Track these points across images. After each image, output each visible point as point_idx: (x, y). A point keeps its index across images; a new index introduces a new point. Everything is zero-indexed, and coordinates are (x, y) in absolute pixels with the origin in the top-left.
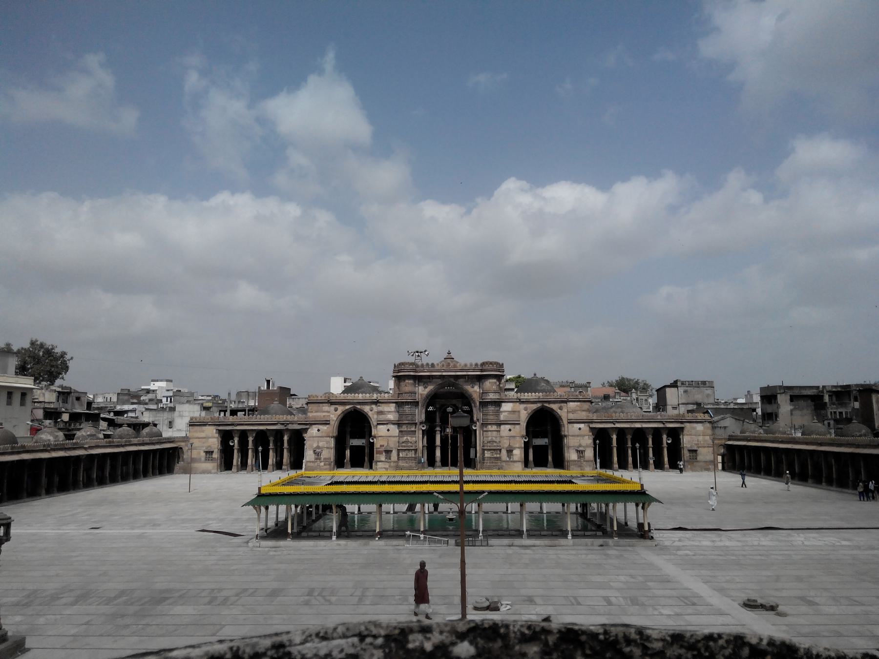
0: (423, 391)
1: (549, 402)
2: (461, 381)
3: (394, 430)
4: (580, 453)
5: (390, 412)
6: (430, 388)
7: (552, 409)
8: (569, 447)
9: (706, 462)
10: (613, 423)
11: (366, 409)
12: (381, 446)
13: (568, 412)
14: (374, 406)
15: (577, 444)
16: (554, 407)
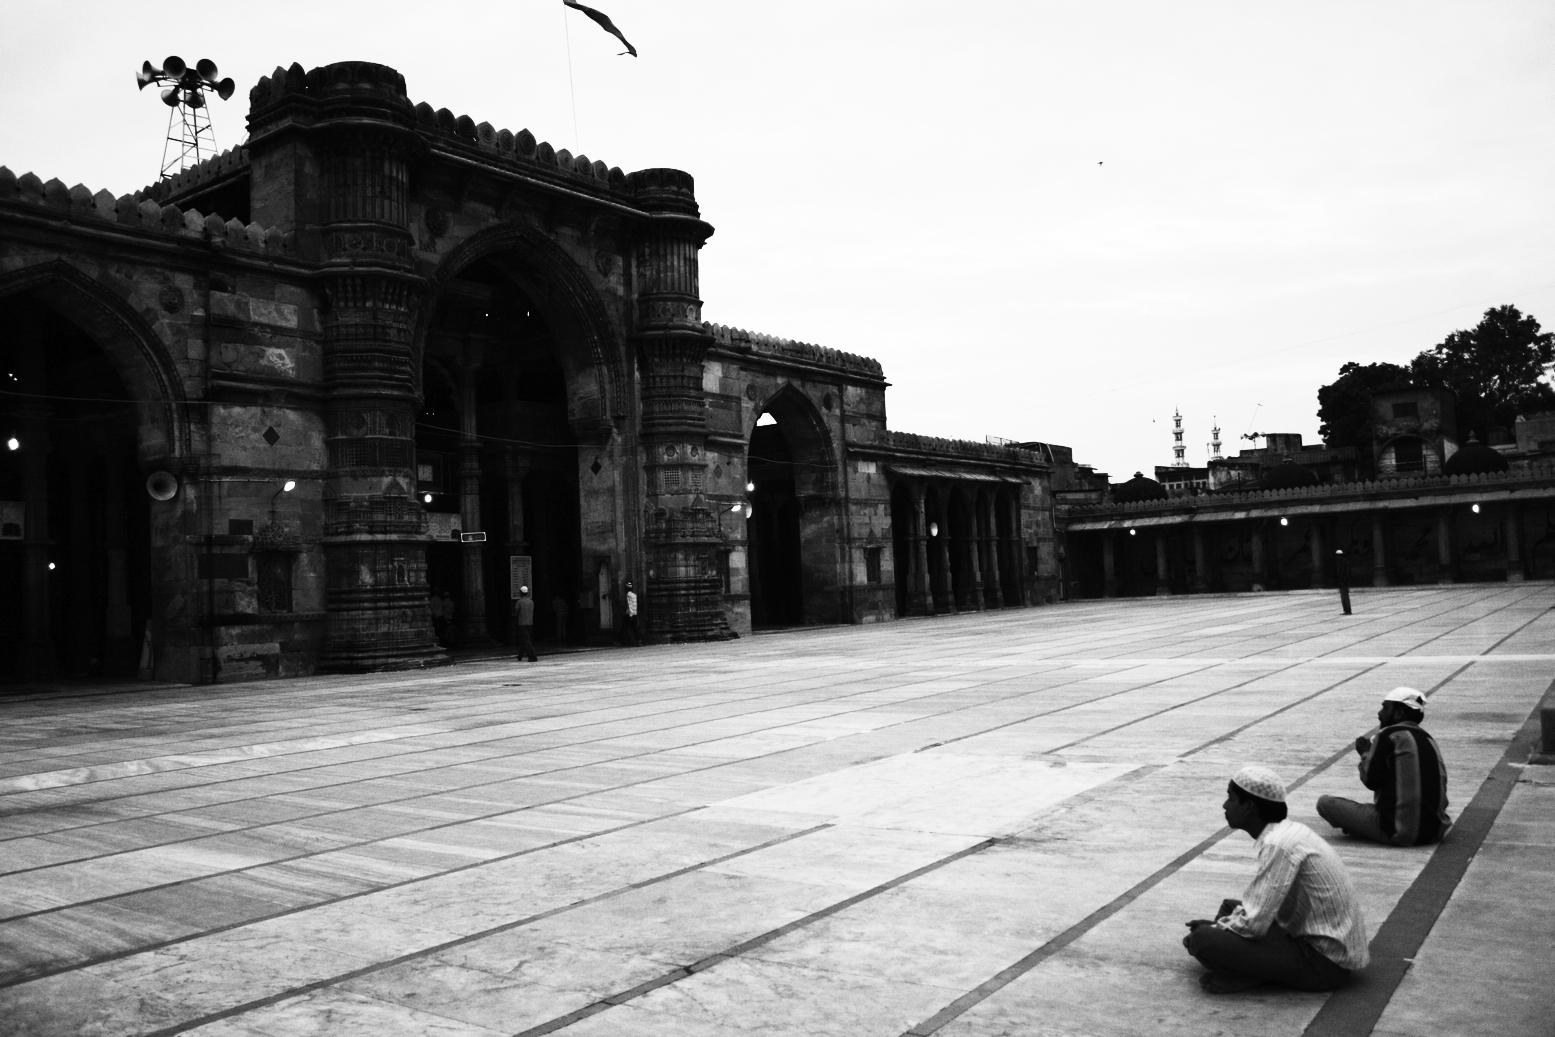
0: (439, 247)
1: (806, 376)
2: (566, 238)
3: (303, 438)
4: (872, 558)
5: (280, 335)
6: (458, 231)
7: (808, 402)
8: (850, 540)
9: (1047, 579)
10: (923, 464)
11: (146, 290)
12: (240, 527)
13: (844, 419)
14: (184, 282)
15: (865, 531)
16: (814, 393)
